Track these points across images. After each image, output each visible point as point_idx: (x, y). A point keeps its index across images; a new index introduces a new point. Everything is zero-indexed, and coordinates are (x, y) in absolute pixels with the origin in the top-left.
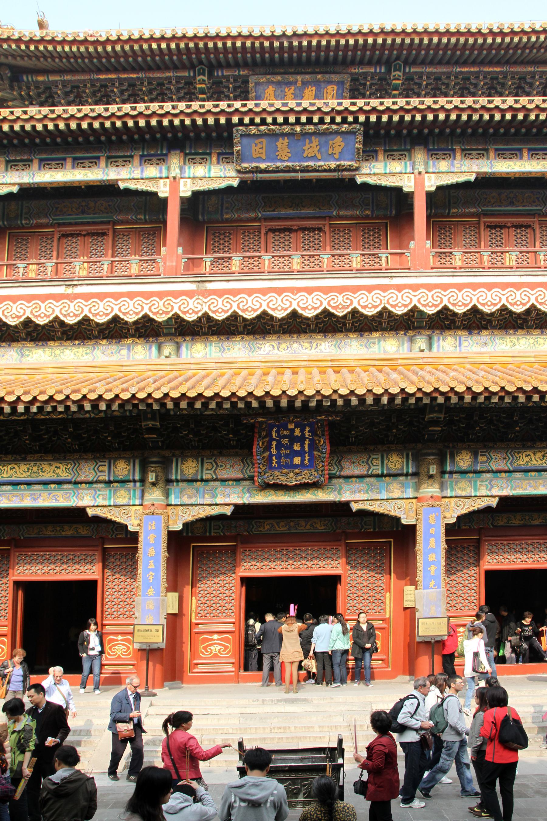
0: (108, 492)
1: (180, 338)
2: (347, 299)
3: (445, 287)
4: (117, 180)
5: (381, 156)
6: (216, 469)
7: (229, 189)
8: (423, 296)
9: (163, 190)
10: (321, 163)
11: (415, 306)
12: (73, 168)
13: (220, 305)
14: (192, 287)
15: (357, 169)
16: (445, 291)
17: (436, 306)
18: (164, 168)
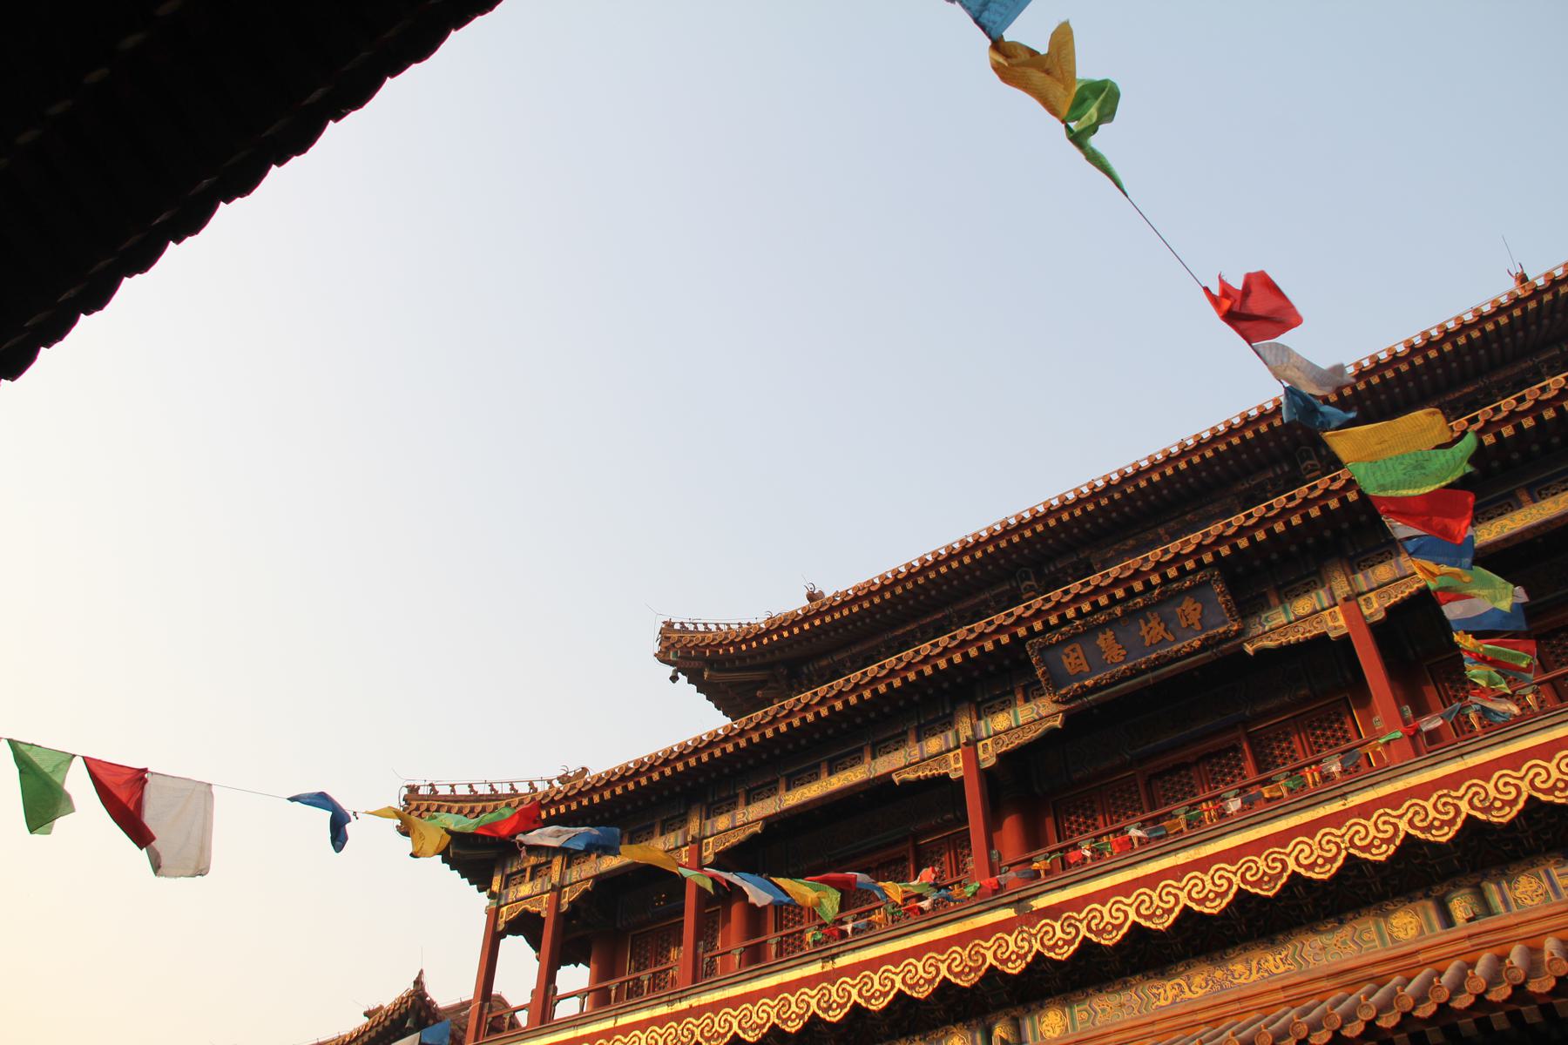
1: (1020, 1008)
2: (1274, 860)
3: (1453, 781)
4: (890, 773)
5: (1274, 600)
7: (1052, 732)
8: (1416, 813)
9: (955, 767)
10: (1175, 648)
11: (1407, 834)
12: (830, 774)
13: (1059, 934)
14: (1008, 913)
15: (1239, 633)
16: (1457, 789)
17: (1451, 823)
18: (950, 734)
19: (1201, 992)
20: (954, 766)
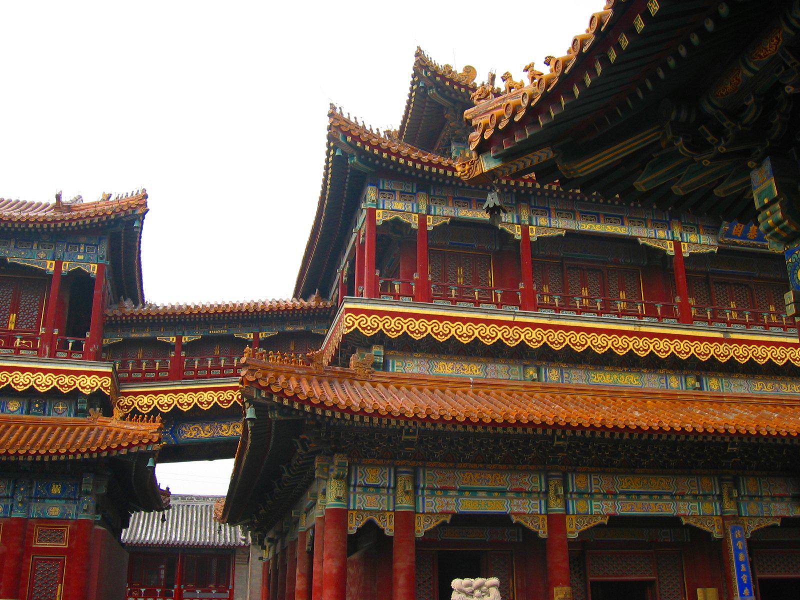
0: (697, 504)
6: (770, 487)
19: (771, 390)
20: (669, 248)
